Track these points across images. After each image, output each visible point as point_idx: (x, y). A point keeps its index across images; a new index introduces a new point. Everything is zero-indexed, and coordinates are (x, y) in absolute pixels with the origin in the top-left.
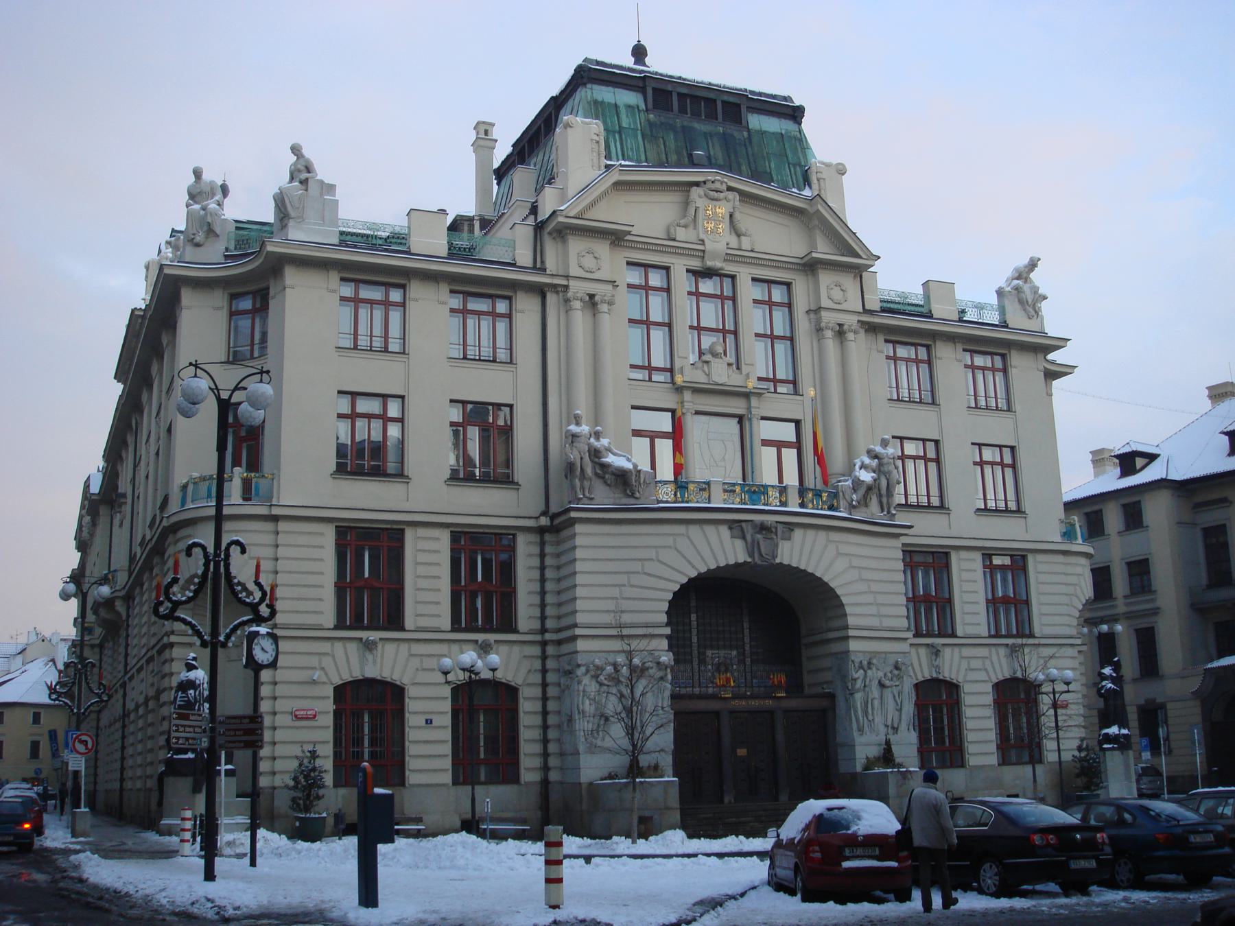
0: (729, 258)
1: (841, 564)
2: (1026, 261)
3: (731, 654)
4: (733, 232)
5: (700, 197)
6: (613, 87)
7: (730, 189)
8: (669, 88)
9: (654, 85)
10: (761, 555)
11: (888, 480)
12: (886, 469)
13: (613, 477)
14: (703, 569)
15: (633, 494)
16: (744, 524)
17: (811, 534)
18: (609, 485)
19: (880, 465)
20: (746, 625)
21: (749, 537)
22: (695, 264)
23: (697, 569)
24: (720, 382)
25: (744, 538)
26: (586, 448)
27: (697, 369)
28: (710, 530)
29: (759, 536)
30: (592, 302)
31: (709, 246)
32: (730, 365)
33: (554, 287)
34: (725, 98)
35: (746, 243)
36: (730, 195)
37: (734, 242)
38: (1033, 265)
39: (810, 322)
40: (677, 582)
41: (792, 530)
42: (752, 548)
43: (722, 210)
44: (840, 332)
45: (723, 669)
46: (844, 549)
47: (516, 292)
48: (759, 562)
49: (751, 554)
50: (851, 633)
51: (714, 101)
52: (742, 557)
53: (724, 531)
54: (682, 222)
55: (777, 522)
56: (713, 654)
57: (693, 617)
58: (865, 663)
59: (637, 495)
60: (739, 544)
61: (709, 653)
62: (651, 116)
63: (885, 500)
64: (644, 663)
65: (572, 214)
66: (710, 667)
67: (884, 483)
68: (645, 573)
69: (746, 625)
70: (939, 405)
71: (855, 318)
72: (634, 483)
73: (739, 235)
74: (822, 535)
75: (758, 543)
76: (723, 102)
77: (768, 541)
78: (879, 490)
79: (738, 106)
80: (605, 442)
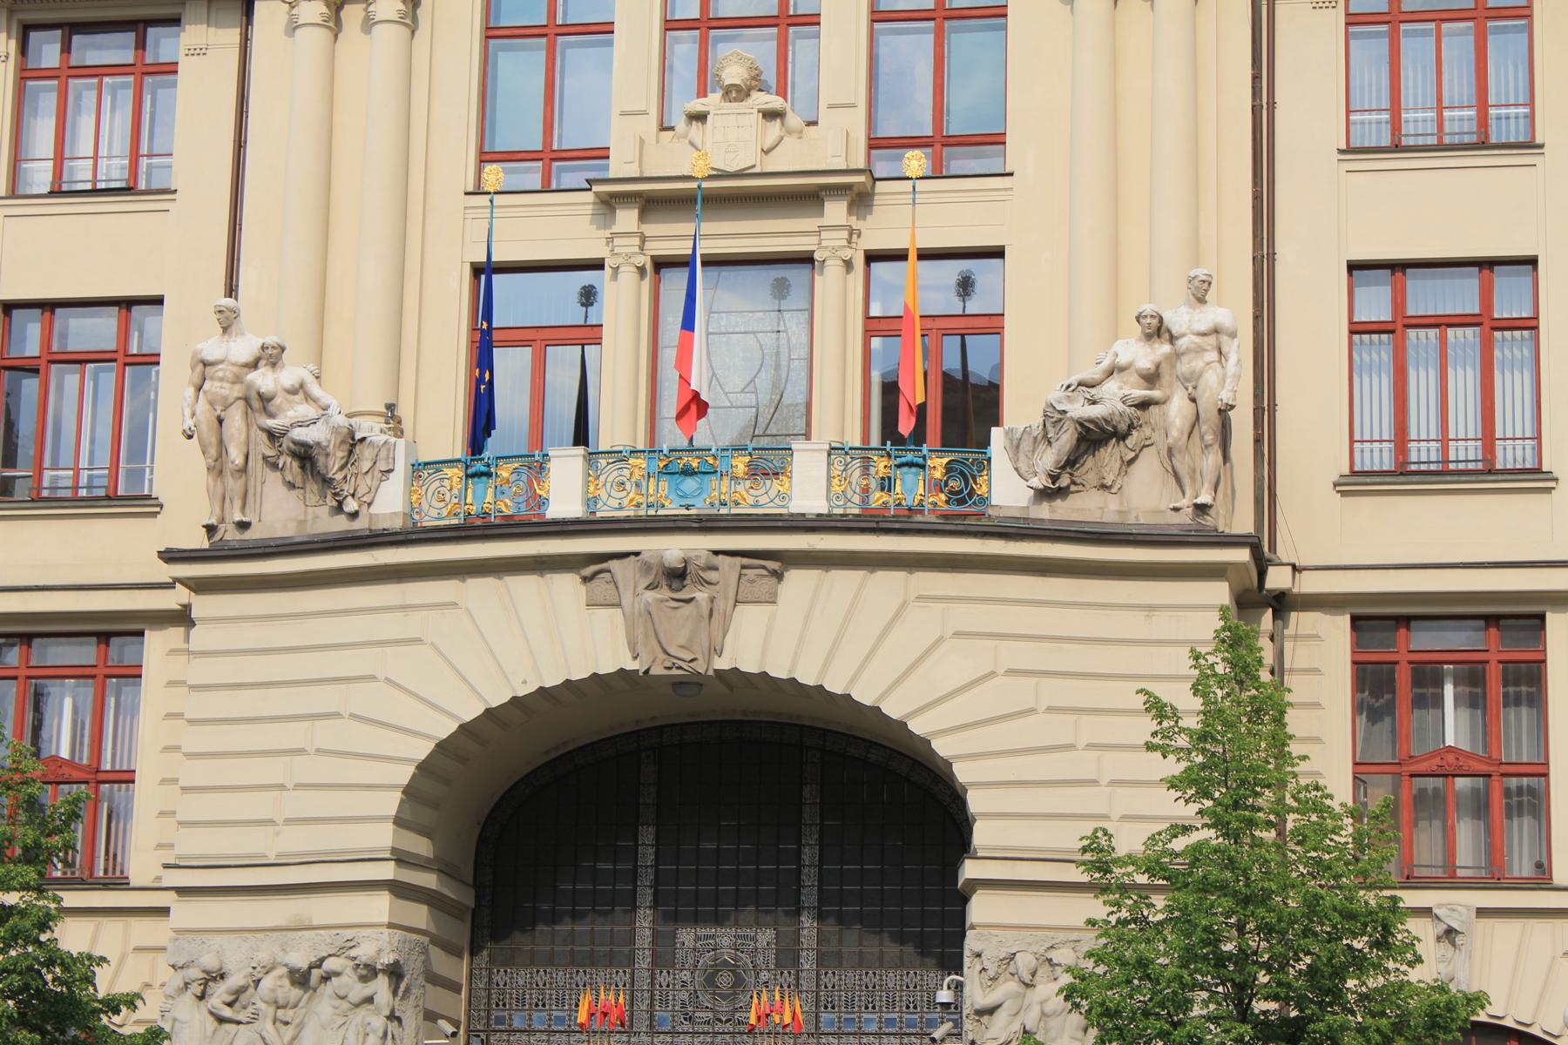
3: (755, 939)
11: (1193, 400)
12: (1184, 367)
13: (295, 464)
15: (340, 503)
16: (614, 565)
18: (291, 486)
20: (809, 855)
21: (627, 599)
24: (732, 167)
25: (619, 605)
26: (237, 391)
27: (679, 137)
28: (524, 586)
29: (650, 596)
32: (771, 115)
41: (778, 576)
42: (643, 627)
45: (725, 980)
47: (183, 4)
48: (657, 670)
53: (567, 585)
55: (716, 553)
56: (698, 939)
57: (647, 835)
58: (1024, 962)
59: (351, 505)
61: (686, 936)
64: (322, 960)
66: (686, 975)
67: (1177, 410)
68: (353, 716)
69: (809, 855)
72: (339, 476)
77: (687, 609)
80: (289, 375)
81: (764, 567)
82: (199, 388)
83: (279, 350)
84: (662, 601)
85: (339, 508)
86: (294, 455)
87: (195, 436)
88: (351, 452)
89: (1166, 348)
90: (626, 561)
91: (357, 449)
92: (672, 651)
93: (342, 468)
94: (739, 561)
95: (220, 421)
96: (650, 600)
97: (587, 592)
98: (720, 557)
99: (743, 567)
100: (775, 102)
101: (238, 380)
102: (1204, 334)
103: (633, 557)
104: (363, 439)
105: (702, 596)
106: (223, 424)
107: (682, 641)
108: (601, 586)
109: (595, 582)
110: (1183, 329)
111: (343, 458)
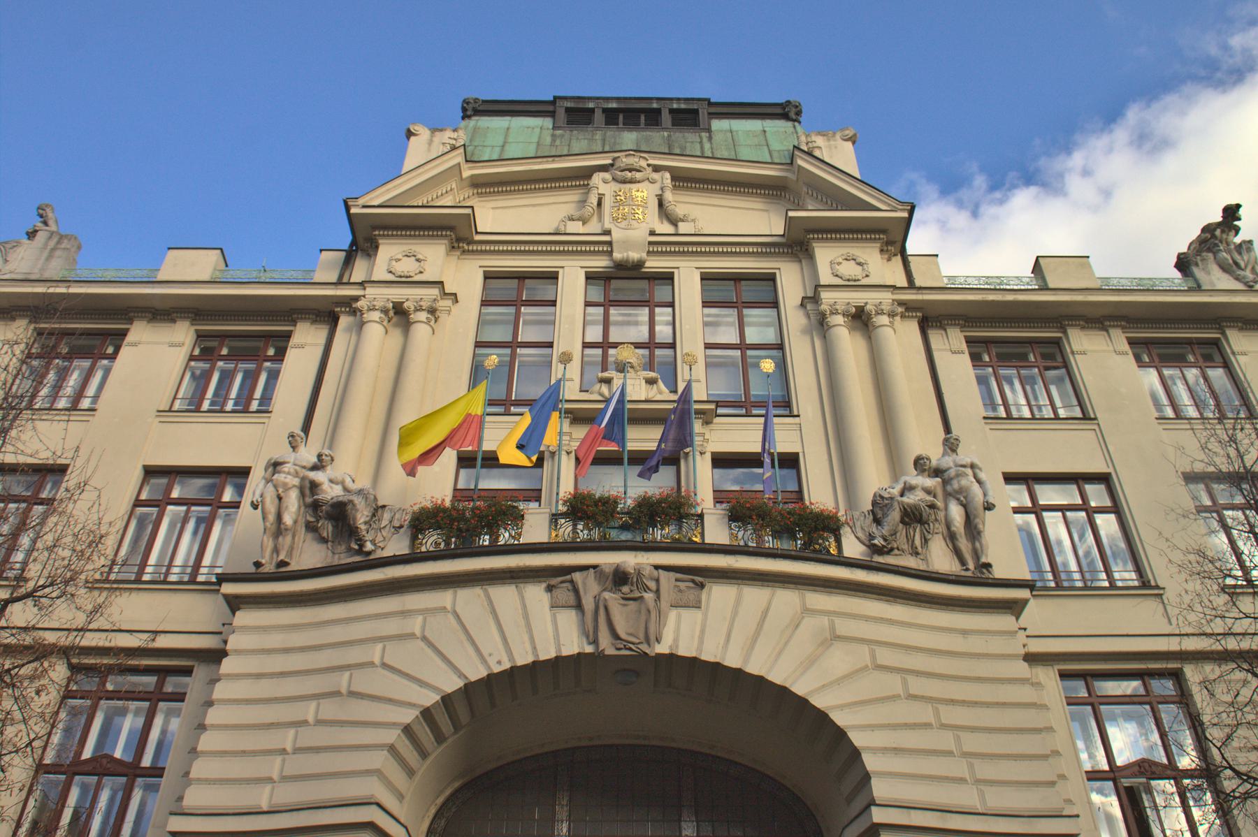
0: (657, 246)
1: (839, 660)
2: (1217, 217)
4: (665, 222)
5: (605, 182)
6: (512, 116)
7: (656, 169)
8: (591, 105)
9: (569, 104)
10: (616, 636)
11: (965, 506)
12: (955, 485)
14: (476, 673)
15: (361, 546)
16: (577, 576)
17: (755, 596)
18: (324, 540)
19: (945, 482)
22: (600, 263)
23: (461, 675)
25: (579, 606)
26: (296, 481)
28: (504, 595)
29: (607, 595)
30: (400, 315)
31: (617, 235)
33: (349, 304)
34: (675, 106)
35: (682, 227)
36: (656, 176)
37: (667, 228)
38: (1231, 213)
39: (809, 317)
40: (412, 705)
41: (702, 586)
43: (644, 193)
44: (861, 319)
46: (845, 627)
47: (295, 326)
48: (610, 651)
49: (595, 642)
50: (878, 816)
51: (658, 111)
52: (573, 644)
53: (536, 594)
54: (577, 214)
55: (657, 567)
60: (568, 619)
62: (558, 132)
63: (964, 544)
65: (376, 203)
70: (1095, 419)
71: (886, 297)
72: (363, 527)
73: (674, 222)
74: (787, 599)
75: (606, 608)
76: (672, 111)
78: (948, 525)
79: (696, 112)
81: (693, 581)
82: (268, 481)
83: (329, 458)
84: (616, 599)
85: (360, 551)
86: (330, 517)
87: (260, 507)
88: (374, 515)
89: (939, 480)
90: (585, 573)
91: (380, 511)
92: (623, 635)
93: (366, 523)
94: (673, 575)
95: (280, 498)
96: (607, 597)
97: (551, 597)
98: (660, 571)
99: (677, 580)
100: (652, 374)
101: (296, 474)
102: (964, 466)
103: (592, 570)
104: (384, 506)
105: (649, 596)
106: (282, 501)
107: (631, 631)
108: (564, 594)
109: (556, 592)
110: (951, 464)
111: (367, 516)
